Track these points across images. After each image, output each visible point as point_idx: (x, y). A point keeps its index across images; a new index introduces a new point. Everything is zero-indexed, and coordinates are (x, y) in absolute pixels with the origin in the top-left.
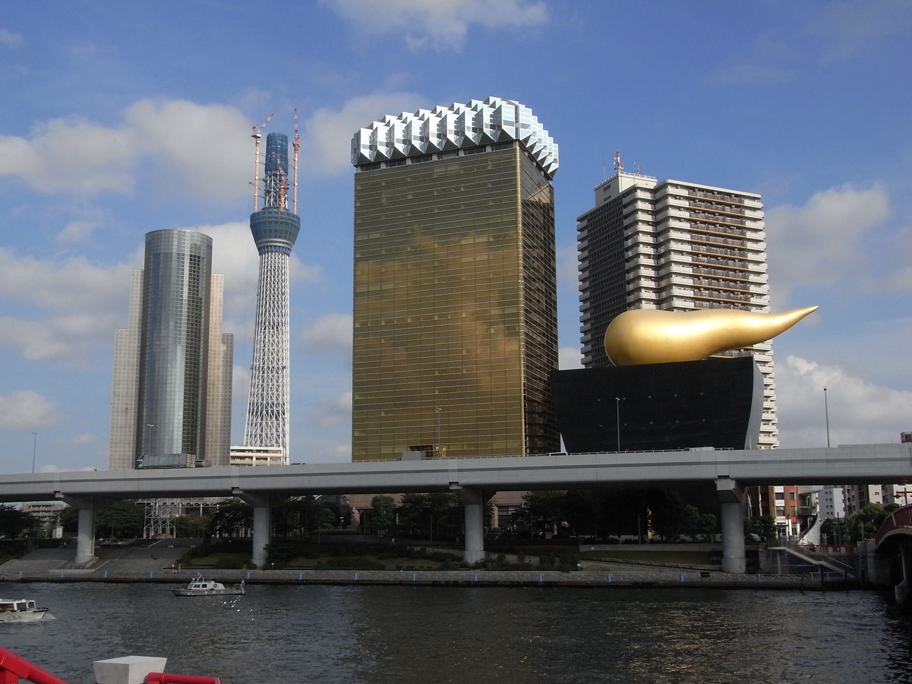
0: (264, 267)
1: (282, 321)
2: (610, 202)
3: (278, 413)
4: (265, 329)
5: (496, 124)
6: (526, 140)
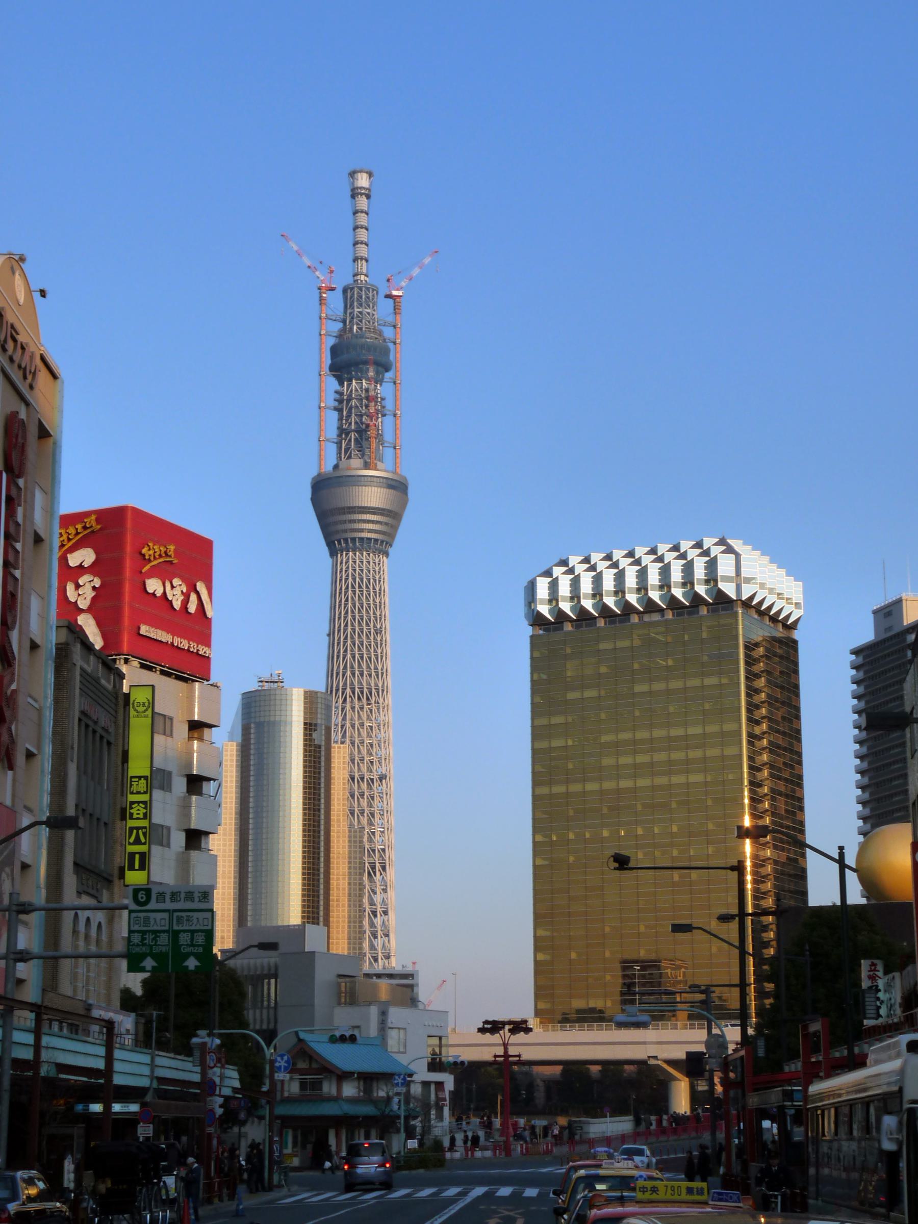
0: (341, 580)
1: (376, 685)
2: (891, 638)
3: (373, 868)
4: (345, 701)
5: (712, 578)
6: (752, 598)
